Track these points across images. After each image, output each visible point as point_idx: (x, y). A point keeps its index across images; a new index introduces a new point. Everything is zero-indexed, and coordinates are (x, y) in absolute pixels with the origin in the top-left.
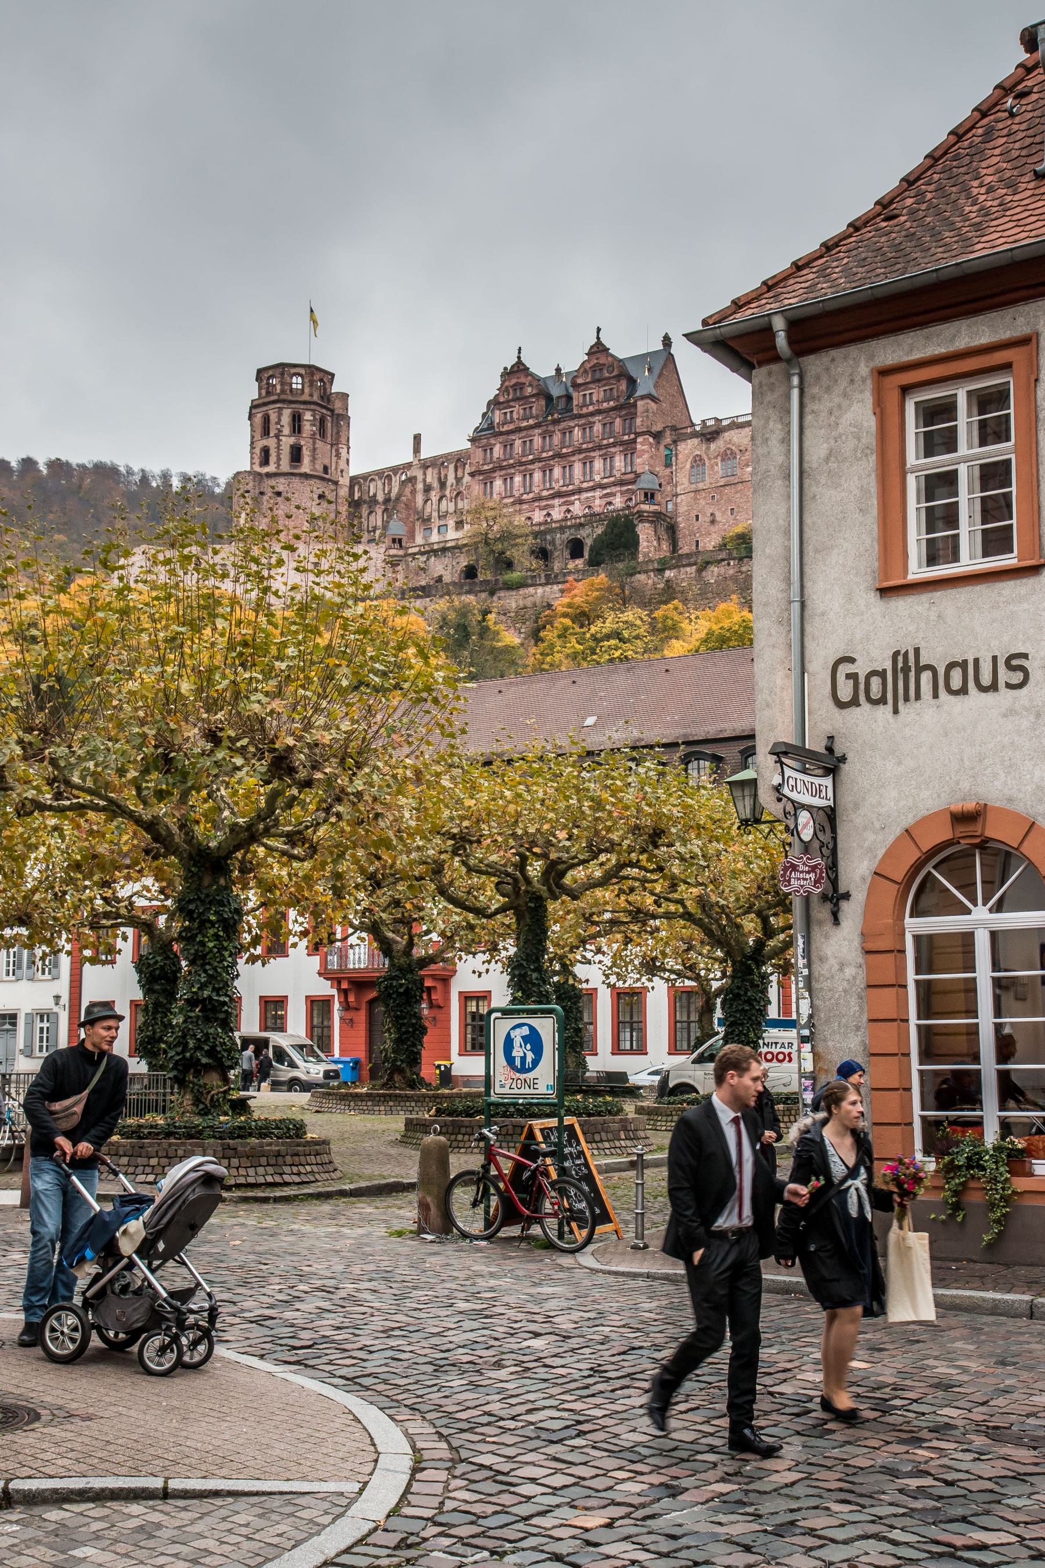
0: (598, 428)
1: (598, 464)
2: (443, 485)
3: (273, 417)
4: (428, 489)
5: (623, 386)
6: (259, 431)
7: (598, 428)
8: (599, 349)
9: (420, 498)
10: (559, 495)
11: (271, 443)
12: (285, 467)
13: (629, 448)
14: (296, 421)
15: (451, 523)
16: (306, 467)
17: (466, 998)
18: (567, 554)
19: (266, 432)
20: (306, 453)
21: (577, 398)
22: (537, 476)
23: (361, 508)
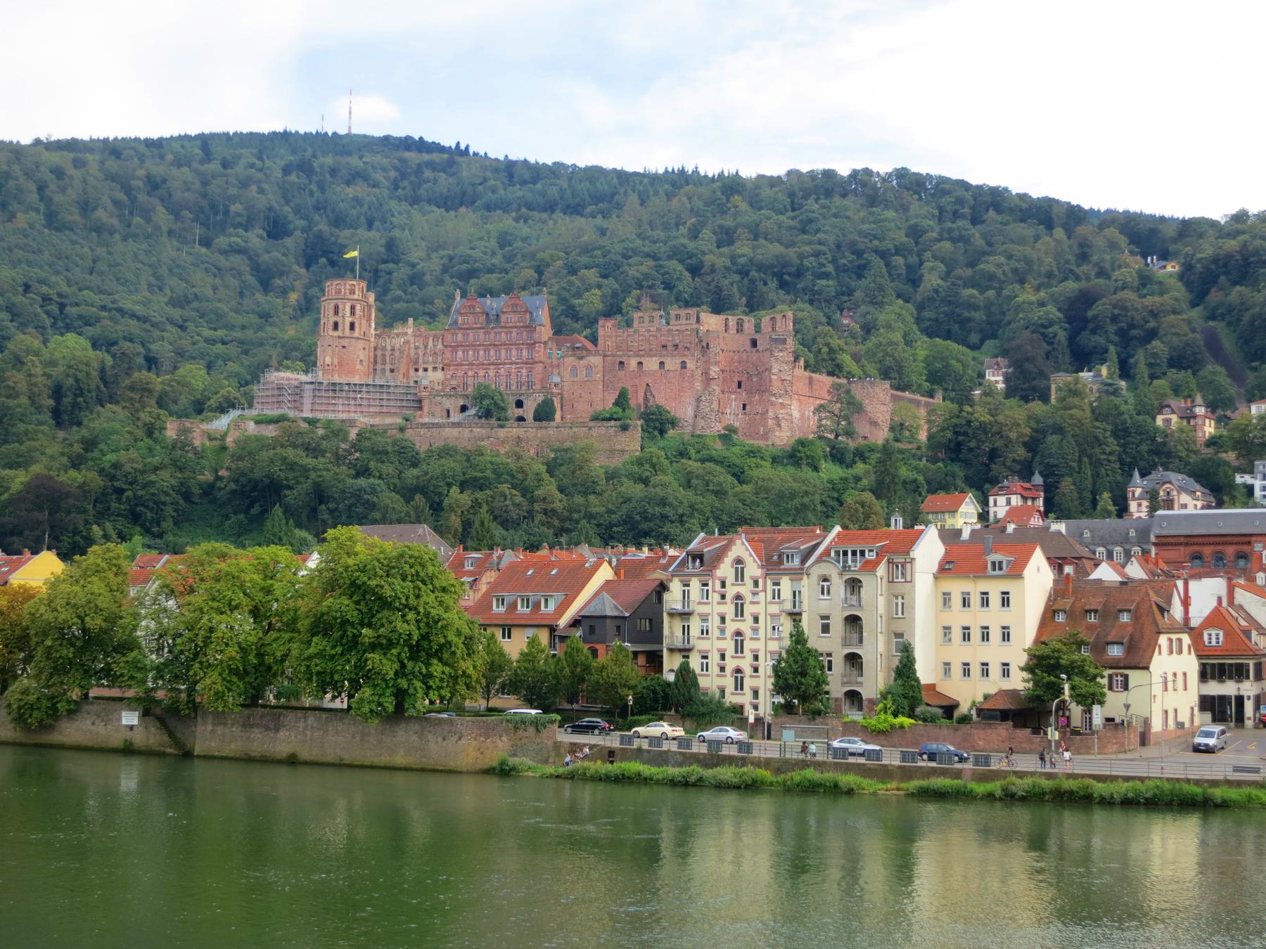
0: (514, 334)
1: (514, 352)
2: (426, 347)
3: (341, 307)
4: (417, 348)
5: (528, 316)
7: (514, 334)
10: (493, 364)
11: (339, 319)
13: (531, 346)
14: (353, 308)
16: (356, 334)
19: (336, 313)
20: (357, 325)
21: (503, 318)
22: (481, 353)
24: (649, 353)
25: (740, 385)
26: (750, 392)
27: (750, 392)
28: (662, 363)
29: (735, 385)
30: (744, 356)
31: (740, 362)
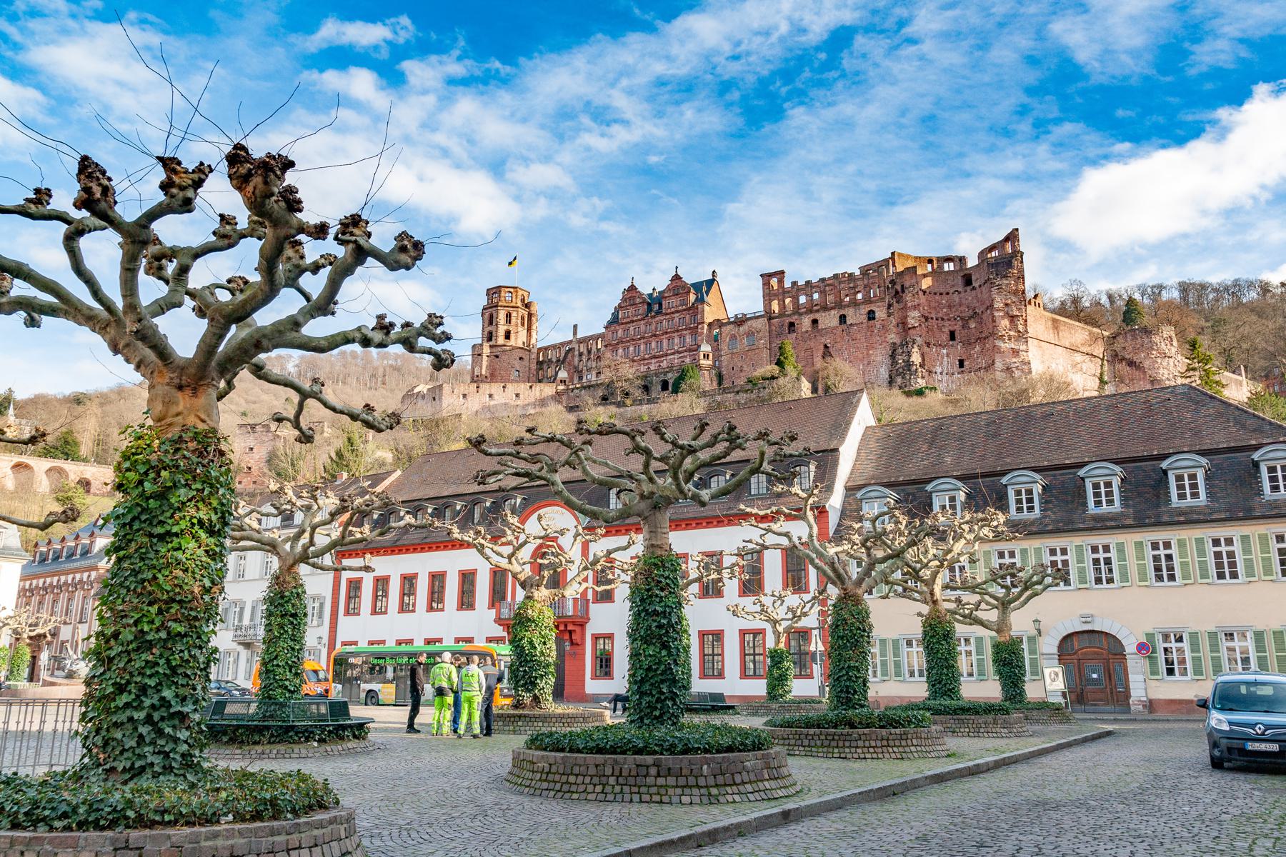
0: (676, 320)
1: (677, 340)
2: (589, 352)
4: (581, 354)
6: (487, 322)
7: (676, 320)
8: (677, 277)
9: (576, 359)
12: (501, 340)
14: (509, 316)
15: (594, 373)
17: (596, 638)
18: (659, 388)
19: (491, 323)
22: (642, 347)
23: (541, 366)
24: (825, 308)
25: (952, 336)
26: (968, 344)
27: (968, 344)
28: (843, 319)
29: (945, 337)
30: (956, 297)
31: (950, 307)
